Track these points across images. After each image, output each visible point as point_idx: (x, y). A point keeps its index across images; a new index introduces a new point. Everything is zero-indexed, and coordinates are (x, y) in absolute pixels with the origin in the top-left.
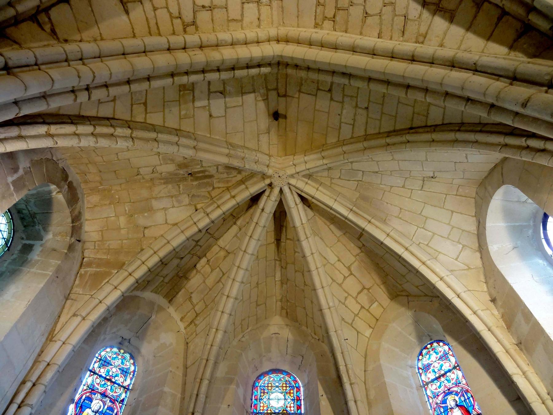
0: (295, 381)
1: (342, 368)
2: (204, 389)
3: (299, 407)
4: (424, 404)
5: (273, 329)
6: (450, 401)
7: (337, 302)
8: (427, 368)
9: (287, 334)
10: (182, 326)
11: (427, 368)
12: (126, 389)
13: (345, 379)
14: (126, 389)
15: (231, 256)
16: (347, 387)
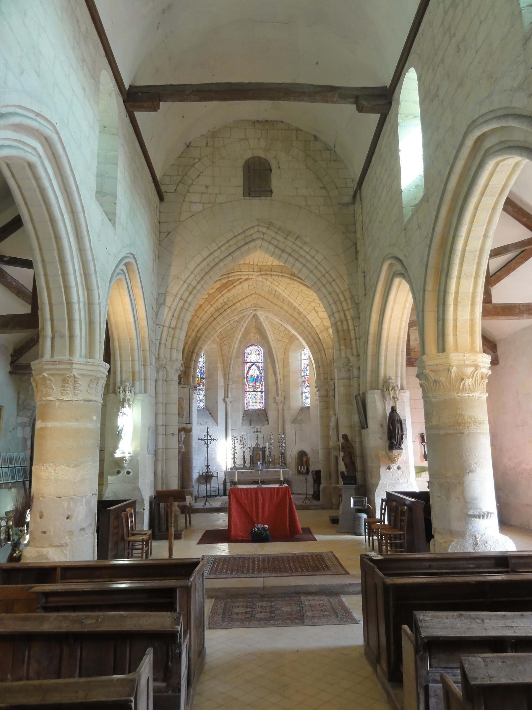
0: (260, 350)
1: (276, 359)
2: (231, 367)
3: (261, 360)
4: (301, 366)
5: (252, 335)
6: (308, 368)
7: (276, 335)
8: (305, 354)
9: (258, 337)
10: (218, 339)
11: (305, 354)
12: (203, 362)
13: (276, 362)
14: (203, 362)
15: (236, 323)
16: (277, 365)
